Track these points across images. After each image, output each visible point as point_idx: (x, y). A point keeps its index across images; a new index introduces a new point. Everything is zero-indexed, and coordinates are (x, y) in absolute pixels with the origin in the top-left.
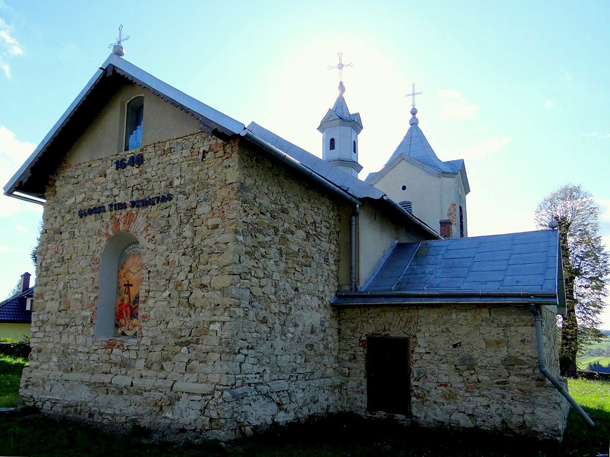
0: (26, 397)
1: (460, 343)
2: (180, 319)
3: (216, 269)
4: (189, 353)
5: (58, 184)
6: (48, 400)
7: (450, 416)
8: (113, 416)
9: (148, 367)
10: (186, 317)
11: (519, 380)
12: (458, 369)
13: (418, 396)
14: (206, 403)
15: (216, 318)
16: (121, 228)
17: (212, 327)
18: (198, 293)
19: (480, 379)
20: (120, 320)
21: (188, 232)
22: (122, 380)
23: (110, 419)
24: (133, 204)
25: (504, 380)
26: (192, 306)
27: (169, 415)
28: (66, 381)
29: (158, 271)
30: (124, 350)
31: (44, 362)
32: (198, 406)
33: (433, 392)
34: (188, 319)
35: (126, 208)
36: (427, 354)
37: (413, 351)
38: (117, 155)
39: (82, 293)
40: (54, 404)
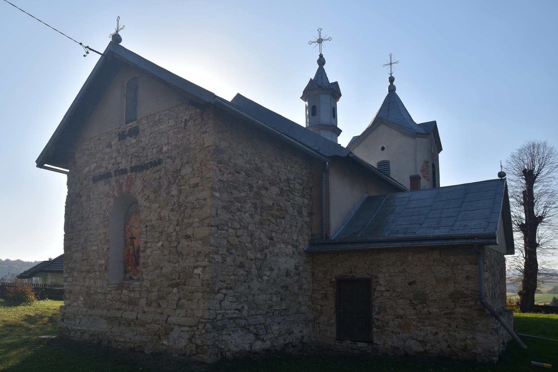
0: (63, 328)
1: (414, 281)
2: (171, 265)
3: (198, 222)
4: (179, 292)
5: (77, 156)
6: (78, 331)
7: (404, 343)
8: (125, 342)
9: (149, 304)
10: (175, 263)
11: (463, 311)
12: (413, 303)
13: (378, 327)
14: (193, 333)
15: (199, 263)
16: (124, 190)
17: (196, 271)
18: (184, 243)
19: (431, 311)
20: (128, 267)
21: (175, 192)
22: (130, 315)
23: (123, 344)
24: (133, 169)
25: (451, 311)
26: (180, 254)
27: (165, 342)
28: (90, 315)
29: (152, 225)
30: (130, 291)
32: (187, 336)
33: (391, 323)
34: (176, 265)
35: (127, 173)
36: (387, 292)
37: (375, 290)
38: (119, 128)
39: (98, 245)
40: (83, 332)
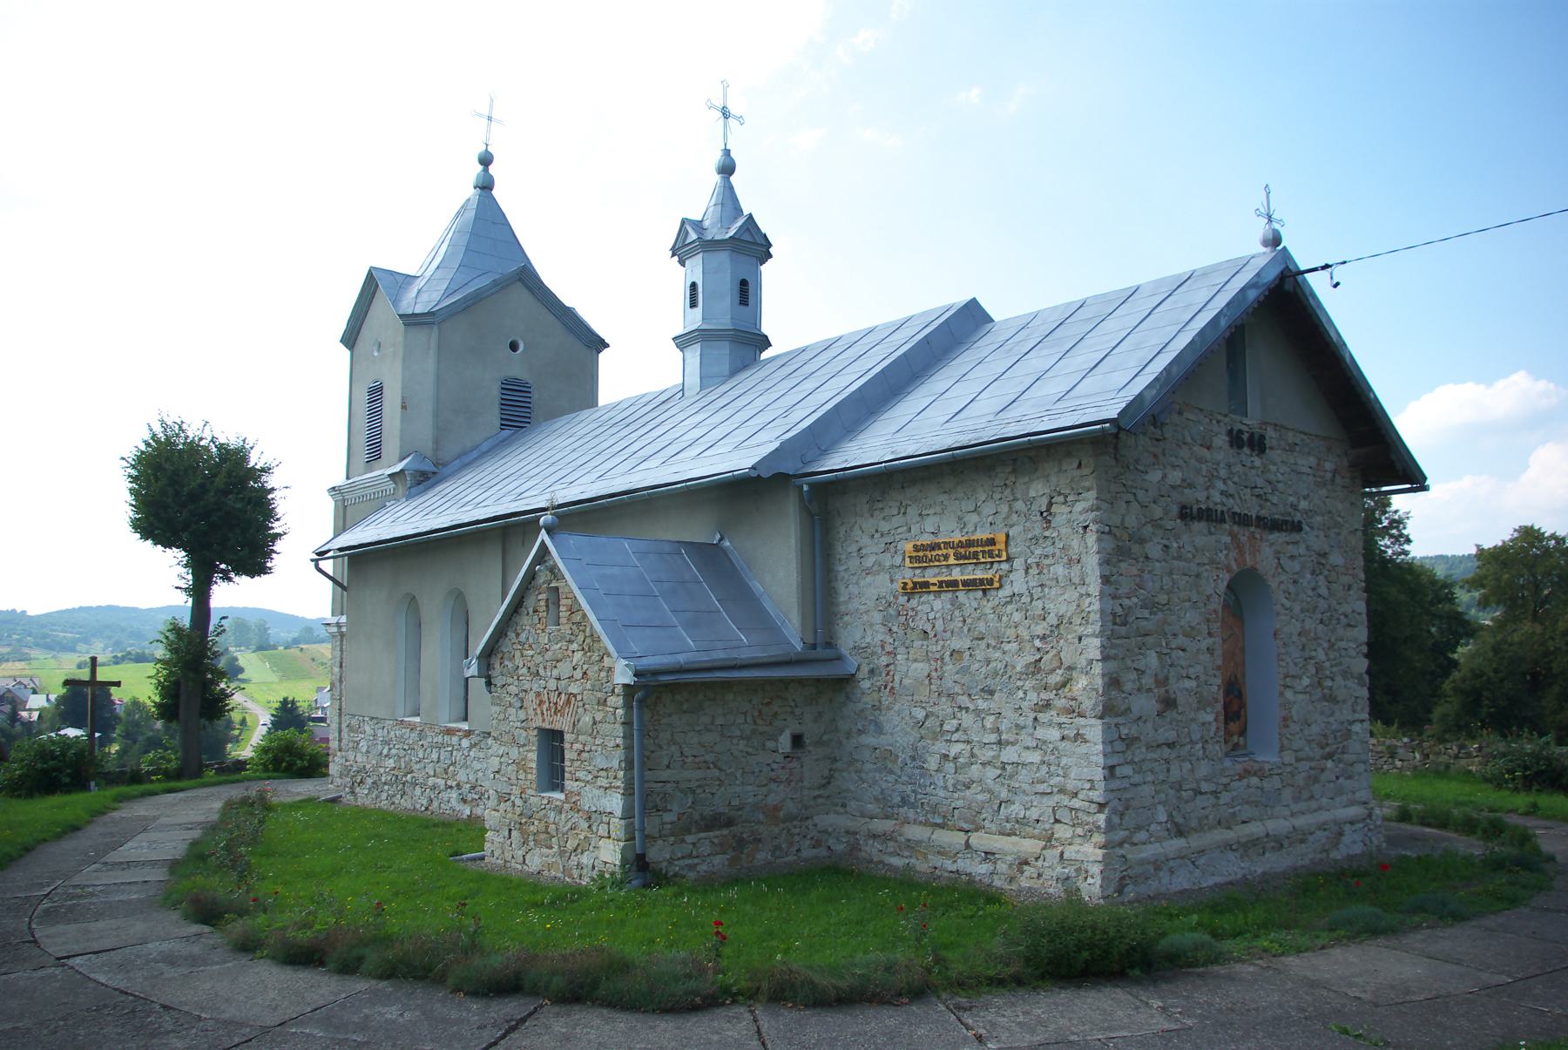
31: (1139, 828)
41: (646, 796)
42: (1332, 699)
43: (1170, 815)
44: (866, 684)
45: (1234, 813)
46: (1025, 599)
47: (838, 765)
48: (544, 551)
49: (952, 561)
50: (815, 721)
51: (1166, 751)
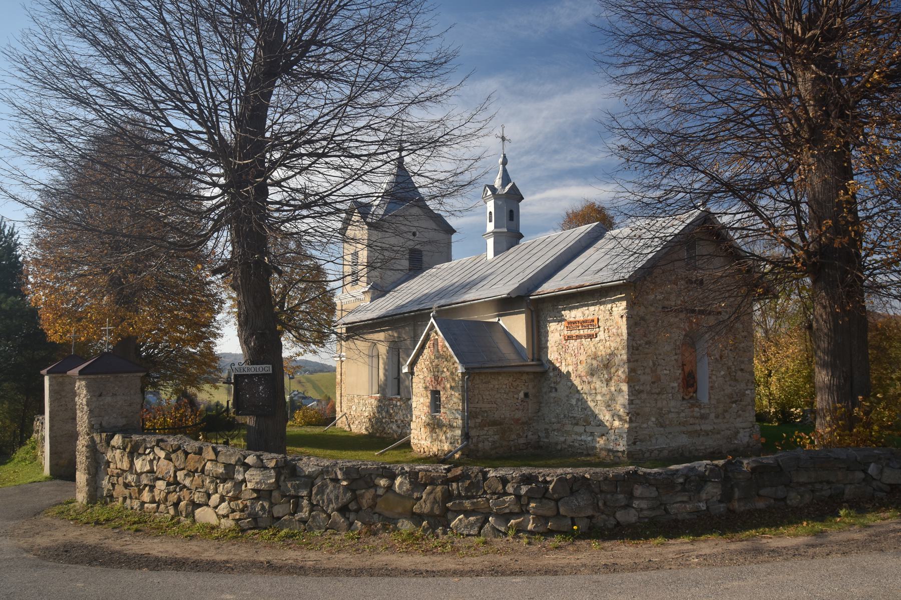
9: (717, 417)
17: (747, 392)
18: (739, 373)
22: (707, 427)
26: (736, 380)
27: (736, 442)
31: (643, 423)
32: (748, 434)
41: (470, 412)
42: (736, 380)
43: (657, 419)
44: (551, 374)
45: (686, 421)
46: (604, 341)
47: (542, 405)
48: (432, 326)
49: (580, 328)
50: (533, 388)
51: (656, 396)
